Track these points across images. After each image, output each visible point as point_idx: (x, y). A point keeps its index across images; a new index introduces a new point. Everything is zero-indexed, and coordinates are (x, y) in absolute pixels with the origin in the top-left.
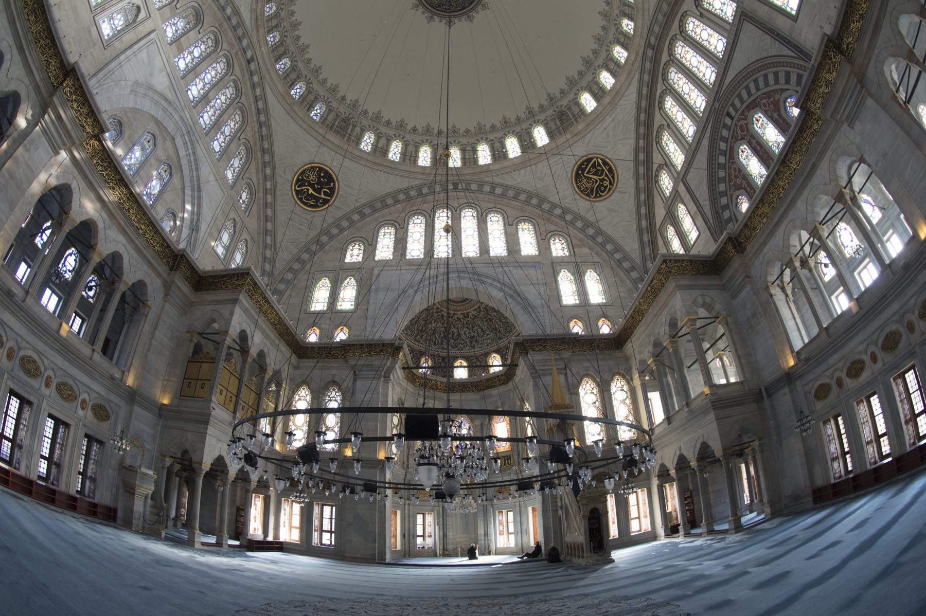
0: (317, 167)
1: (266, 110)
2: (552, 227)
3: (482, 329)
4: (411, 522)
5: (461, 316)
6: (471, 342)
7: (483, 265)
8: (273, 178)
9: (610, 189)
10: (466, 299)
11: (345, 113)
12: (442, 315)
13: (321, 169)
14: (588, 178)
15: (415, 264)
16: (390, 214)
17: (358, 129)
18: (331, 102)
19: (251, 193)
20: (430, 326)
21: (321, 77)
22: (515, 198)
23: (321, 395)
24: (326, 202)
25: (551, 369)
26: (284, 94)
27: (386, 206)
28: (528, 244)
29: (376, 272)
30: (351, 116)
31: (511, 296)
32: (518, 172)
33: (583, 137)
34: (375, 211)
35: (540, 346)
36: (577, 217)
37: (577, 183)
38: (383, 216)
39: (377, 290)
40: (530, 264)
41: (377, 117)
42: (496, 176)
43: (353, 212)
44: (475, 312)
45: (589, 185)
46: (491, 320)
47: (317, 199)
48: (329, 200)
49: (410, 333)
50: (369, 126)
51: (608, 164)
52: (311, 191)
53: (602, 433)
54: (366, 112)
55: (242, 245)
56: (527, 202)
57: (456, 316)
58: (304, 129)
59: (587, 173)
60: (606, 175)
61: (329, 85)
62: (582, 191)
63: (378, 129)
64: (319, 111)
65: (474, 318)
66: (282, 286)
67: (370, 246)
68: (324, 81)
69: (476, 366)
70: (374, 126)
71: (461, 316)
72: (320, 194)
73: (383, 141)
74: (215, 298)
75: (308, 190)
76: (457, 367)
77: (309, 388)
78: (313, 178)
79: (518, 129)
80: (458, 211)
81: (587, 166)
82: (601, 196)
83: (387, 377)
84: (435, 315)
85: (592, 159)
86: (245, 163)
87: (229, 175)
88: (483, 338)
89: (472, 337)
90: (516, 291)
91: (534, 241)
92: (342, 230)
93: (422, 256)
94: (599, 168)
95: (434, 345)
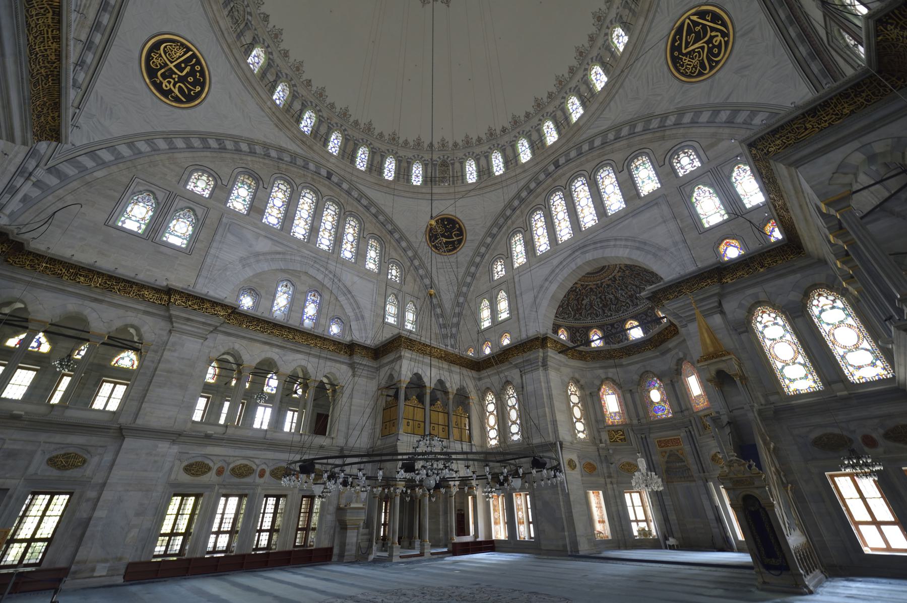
1: (372, 203)
2: (675, 142)
3: (636, 286)
4: (619, 503)
5: (609, 282)
6: (632, 301)
7: (602, 230)
9: (727, 43)
10: (604, 267)
11: (439, 158)
12: (591, 288)
14: (689, 53)
15: (546, 256)
16: (513, 223)
17: (457, 165)
18: (422, 157)
19: (400, 266)
21: (401, 141)
22: (617, 138)
23: (502, 396)
24: (460, 241)
25: (694, 314)
26: (376, 182)
27: (508, 218)
28: (646, 181)
29: (516, 280)
30: (446, 157)
31: (638, 248)
32: (608, 108)
33: (658, 5)
34: (500, 227)
36: (698, 111)
37: (678, 70)
38: (509, 228)
39: (521, 294)
40: (651, 204)
41: (468, 142)
42: (589, 129)
43: (484, 238)
44: (620, 274)
45: (695, 62)
48: (462, 239)
49: (566, 316)
51: (707, 12)
52: (444, 240)
54: (455, 145)
55: (410, 306)
56: (632, 134)
57: (604, 284)
58: (410, 198)
59: (686, 48)
60: (713, 29)
61: (412, 143)
62: (690, 76)
63: (473, 153)
64: (417, 172)
65: (623, 279)
67: (508, 257)
68: (406, 143)
69: (648, 322)
70: (469, 153)
71: (610, 282)
73: (483, 161)
74: (388, 360)
76: (630, 329)
77: (492, 392)
79: (594, 53)
80: (568, 188)
81: (681, 39)
82: (717, 62)
83: (545, 365)
85: (683, 23)
86: (381, 251)
87: (371, 265)
89: (631, 296)
91: (652, 174)
92: (483, 256)
93: (549, 248)
94: (698, 28)
95: (597, 316)
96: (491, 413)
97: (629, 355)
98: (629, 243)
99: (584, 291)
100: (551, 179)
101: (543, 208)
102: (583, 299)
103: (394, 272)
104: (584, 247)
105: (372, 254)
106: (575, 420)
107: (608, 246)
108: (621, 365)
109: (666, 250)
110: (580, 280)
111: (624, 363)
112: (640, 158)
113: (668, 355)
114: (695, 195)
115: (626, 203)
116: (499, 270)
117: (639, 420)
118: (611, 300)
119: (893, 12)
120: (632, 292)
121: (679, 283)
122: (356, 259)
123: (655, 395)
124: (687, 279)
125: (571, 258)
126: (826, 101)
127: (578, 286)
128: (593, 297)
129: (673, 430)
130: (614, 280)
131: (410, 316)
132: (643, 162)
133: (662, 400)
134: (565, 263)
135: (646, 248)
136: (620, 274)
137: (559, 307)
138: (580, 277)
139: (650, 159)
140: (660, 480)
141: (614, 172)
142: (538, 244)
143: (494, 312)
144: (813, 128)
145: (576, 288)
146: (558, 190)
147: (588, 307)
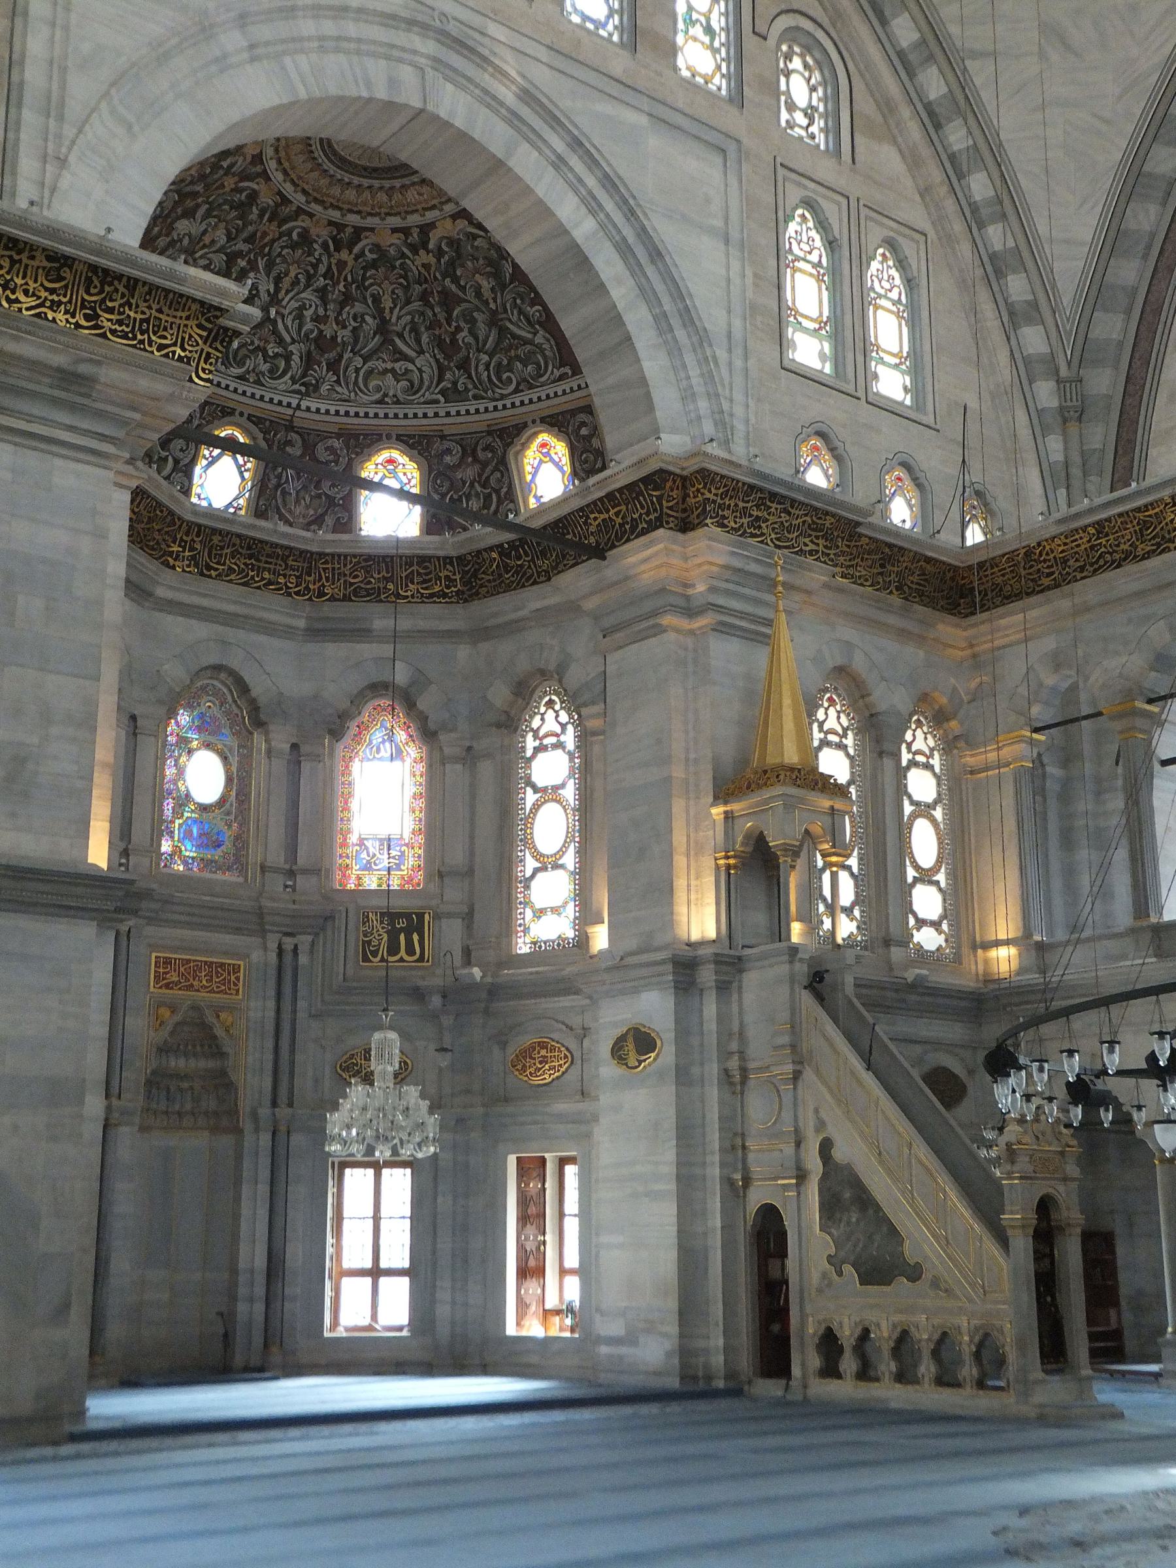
5: (321, 233)
6: (309, 361)
7: (543, 54)
12: (253, 196)
35: (745, 512)
44: (397, 239)
46: (449, 301)
57: (303, 222)
65: (374, 265)
71: (321, 233)
84: (230, 183)
88: (369, 364)
89: (322, 343)
90: (643, 233)
97: (204, 571)
98: (609, 206)
102: (189, 214)
104: (460, 45)
107: (535, 140)
109: (702, 338)
111: (160, 592)
113: (334, 650)
117: (125, 853)
120: (344, 335)
121: (773, 496)
124: (793, 501)
125: (376, 32)
128: (221, 236)
129: (238, 931)
134: (352, 29)
135: (650, 271)
140: (432, 1121)
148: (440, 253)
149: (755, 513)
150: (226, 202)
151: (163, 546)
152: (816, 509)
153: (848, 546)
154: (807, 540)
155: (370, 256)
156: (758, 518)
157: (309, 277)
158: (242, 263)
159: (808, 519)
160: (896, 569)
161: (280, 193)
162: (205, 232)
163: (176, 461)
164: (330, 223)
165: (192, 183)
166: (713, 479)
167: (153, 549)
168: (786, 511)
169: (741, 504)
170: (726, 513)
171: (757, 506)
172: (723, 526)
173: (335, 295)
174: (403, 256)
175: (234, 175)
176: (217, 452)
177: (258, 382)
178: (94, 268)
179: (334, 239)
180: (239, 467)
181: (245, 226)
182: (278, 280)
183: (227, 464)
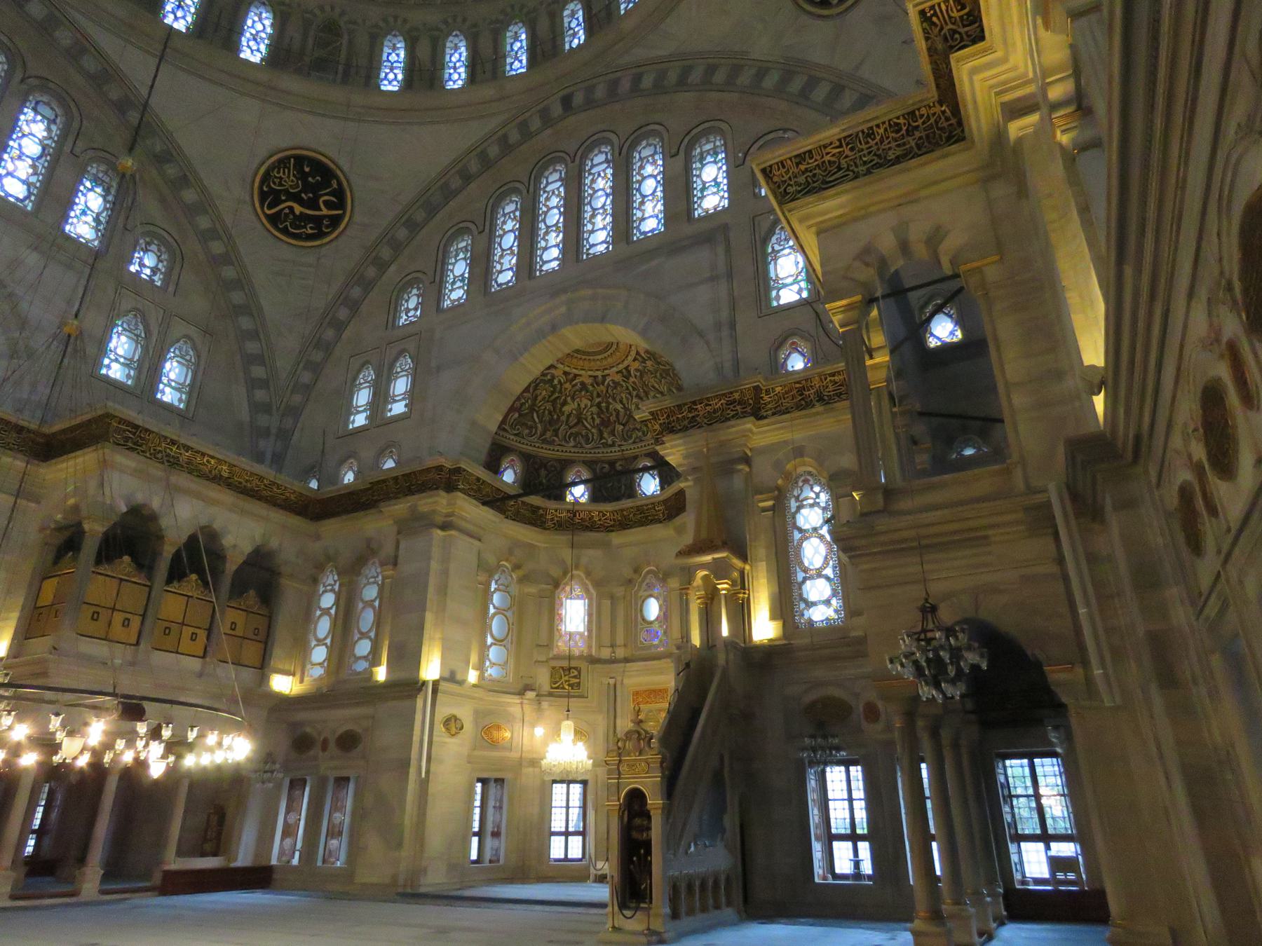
0: (288, 158)
5: (618, 378)
8: (205, 205)
12: (583, 384)
13: (300, 160)
20: (567, 409)
24: (335, 221)
47: (317, 221)
49: (527, 431)
50: (385, 20)
52: (298, 209)
53: (834, 602)
57: (608, 379)
63: (405, 21)
66: (297, 399)
67: (435, 283)
70: (396, 18)
71: (618, 378)
72: (321, 210)
75: (291, 208)
78: (289, 180)
92: (383, 266)
95: (587, 442)
96: (326, 612)
99: (568, 385)
100: (549, 131)
101: (525, 191)
102: (565, 403)
103: (145, 264)
105: (92, 200)
106: (489, 640)
108: (606, 545)
109: (701, 335)
110: (560, 361)
112: (712, 139)
114: (774, 239)
115: (665, 225)
116: (411, 308)
118: (618, 412)
119: (939, 5)
122: (39, 205)
123: (653, 609)
124: (708, 399)
126: (871, 128)
127: (558, 373)
128: (585, 402)
130: (626, 374)
131: (173, 370)
132: (715, 147)
133: (657, 618)
136: (636, 365)
137: (512, 409)
138: (560, 355)
139: (725, 145)
141: (663, 153)
142: (498, 267)
143: (381, 397)
144: (848, 170)
145: (553, 377)
146: (561, 160)
147: (573, 421)
148: (649, 358)
149: (690, 415)
150: (575, 392)
151: (606, 525)
152: (724, 394)
153: (770, 397)
154: (729, 412)
155: (638, 374)
156: (693, 417)
157: (630, 394)
158: (604, 405)
159: (722, 401)
160: (812, 391)
161: (590, 376)
162: (579, 405)
163: (625, 485)
164: (617, 372)
165: (550, 397)
166: (657, 414)
167: (599, 528)
168: (707, 405)
169: (680, 416)
170: (673, 424)
171: (690, 412)
172: (674, 431)
173: (642, 394)
174: (645, 367)
175: (565, 383)
176: (641, 474)
177: (641, 441)
178: (403, 475)
179: (623, 376)
180: (651, 475)
181: (592, 394)
182: (621, 402)
183: (647, 477)
